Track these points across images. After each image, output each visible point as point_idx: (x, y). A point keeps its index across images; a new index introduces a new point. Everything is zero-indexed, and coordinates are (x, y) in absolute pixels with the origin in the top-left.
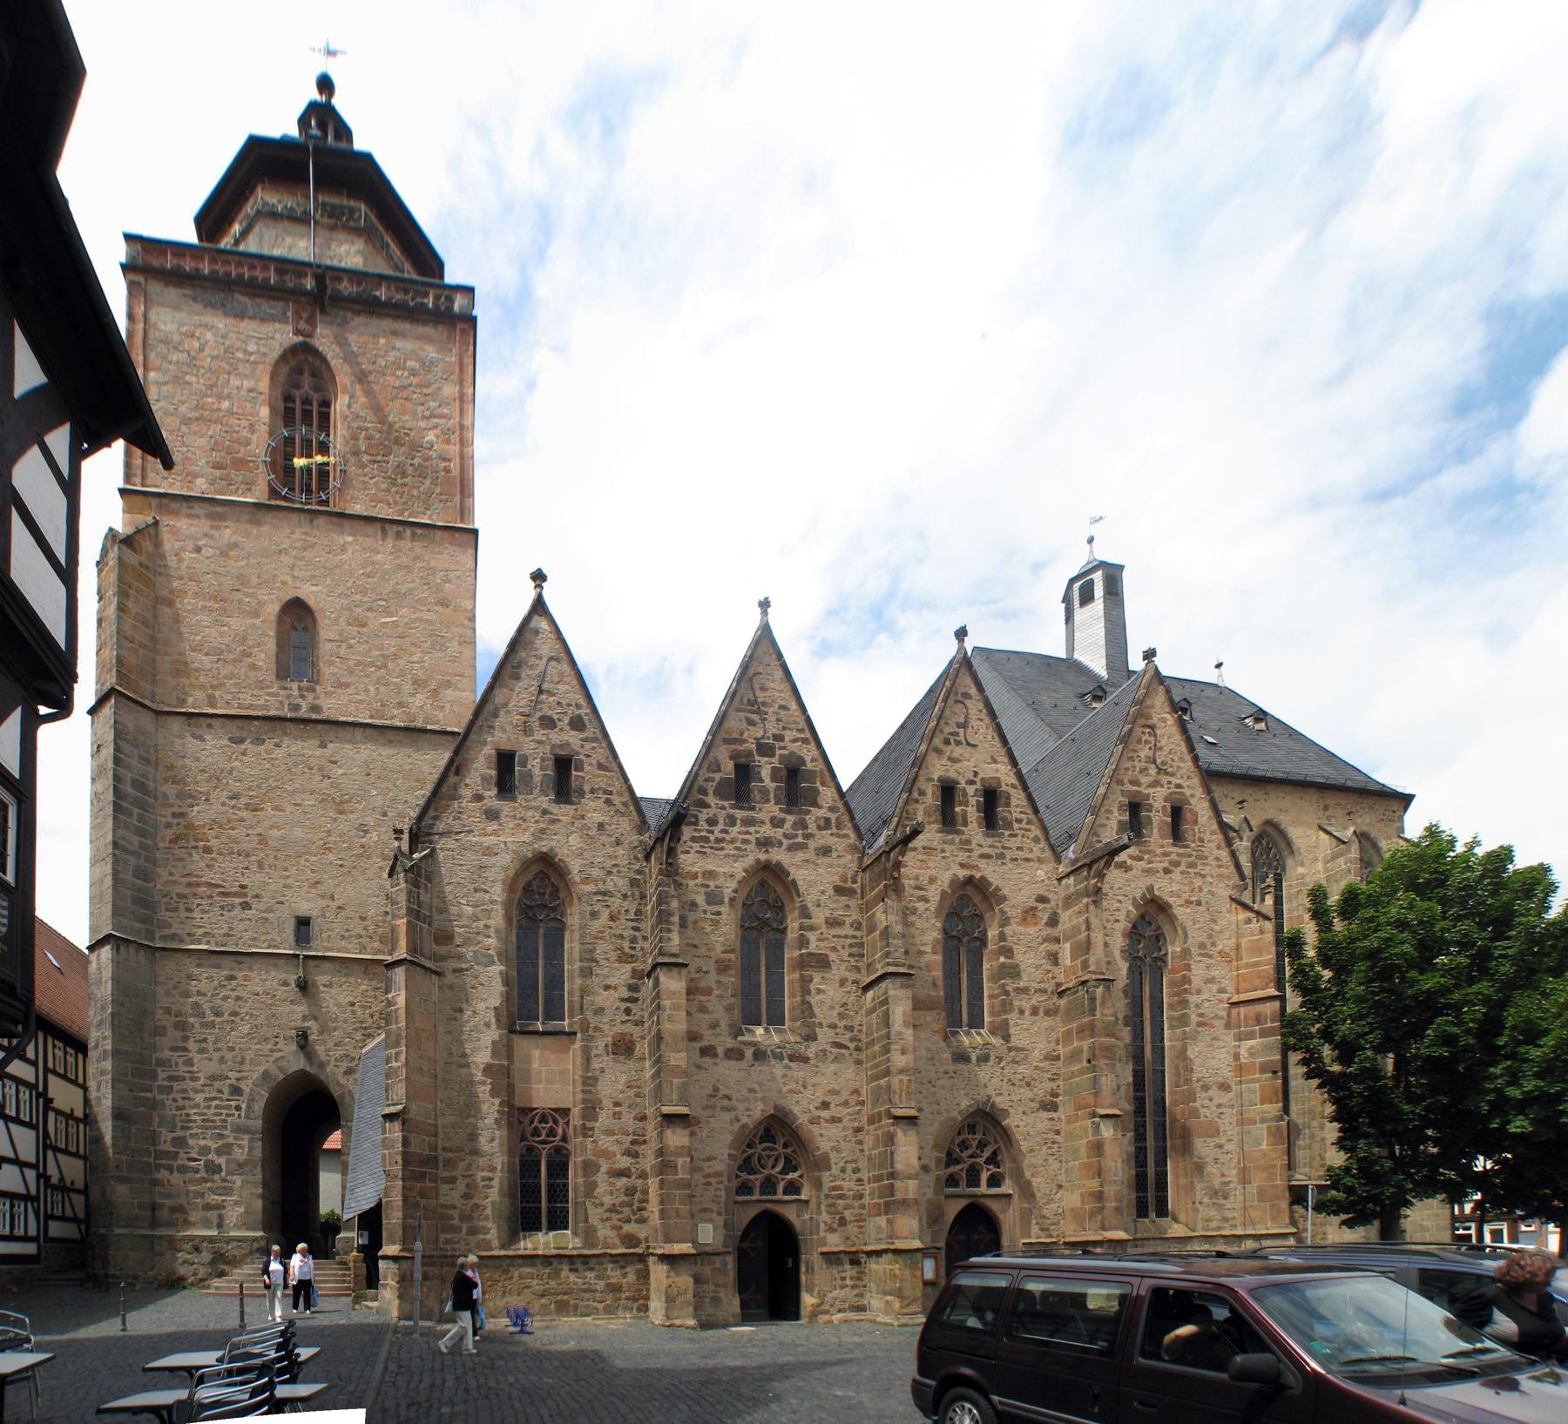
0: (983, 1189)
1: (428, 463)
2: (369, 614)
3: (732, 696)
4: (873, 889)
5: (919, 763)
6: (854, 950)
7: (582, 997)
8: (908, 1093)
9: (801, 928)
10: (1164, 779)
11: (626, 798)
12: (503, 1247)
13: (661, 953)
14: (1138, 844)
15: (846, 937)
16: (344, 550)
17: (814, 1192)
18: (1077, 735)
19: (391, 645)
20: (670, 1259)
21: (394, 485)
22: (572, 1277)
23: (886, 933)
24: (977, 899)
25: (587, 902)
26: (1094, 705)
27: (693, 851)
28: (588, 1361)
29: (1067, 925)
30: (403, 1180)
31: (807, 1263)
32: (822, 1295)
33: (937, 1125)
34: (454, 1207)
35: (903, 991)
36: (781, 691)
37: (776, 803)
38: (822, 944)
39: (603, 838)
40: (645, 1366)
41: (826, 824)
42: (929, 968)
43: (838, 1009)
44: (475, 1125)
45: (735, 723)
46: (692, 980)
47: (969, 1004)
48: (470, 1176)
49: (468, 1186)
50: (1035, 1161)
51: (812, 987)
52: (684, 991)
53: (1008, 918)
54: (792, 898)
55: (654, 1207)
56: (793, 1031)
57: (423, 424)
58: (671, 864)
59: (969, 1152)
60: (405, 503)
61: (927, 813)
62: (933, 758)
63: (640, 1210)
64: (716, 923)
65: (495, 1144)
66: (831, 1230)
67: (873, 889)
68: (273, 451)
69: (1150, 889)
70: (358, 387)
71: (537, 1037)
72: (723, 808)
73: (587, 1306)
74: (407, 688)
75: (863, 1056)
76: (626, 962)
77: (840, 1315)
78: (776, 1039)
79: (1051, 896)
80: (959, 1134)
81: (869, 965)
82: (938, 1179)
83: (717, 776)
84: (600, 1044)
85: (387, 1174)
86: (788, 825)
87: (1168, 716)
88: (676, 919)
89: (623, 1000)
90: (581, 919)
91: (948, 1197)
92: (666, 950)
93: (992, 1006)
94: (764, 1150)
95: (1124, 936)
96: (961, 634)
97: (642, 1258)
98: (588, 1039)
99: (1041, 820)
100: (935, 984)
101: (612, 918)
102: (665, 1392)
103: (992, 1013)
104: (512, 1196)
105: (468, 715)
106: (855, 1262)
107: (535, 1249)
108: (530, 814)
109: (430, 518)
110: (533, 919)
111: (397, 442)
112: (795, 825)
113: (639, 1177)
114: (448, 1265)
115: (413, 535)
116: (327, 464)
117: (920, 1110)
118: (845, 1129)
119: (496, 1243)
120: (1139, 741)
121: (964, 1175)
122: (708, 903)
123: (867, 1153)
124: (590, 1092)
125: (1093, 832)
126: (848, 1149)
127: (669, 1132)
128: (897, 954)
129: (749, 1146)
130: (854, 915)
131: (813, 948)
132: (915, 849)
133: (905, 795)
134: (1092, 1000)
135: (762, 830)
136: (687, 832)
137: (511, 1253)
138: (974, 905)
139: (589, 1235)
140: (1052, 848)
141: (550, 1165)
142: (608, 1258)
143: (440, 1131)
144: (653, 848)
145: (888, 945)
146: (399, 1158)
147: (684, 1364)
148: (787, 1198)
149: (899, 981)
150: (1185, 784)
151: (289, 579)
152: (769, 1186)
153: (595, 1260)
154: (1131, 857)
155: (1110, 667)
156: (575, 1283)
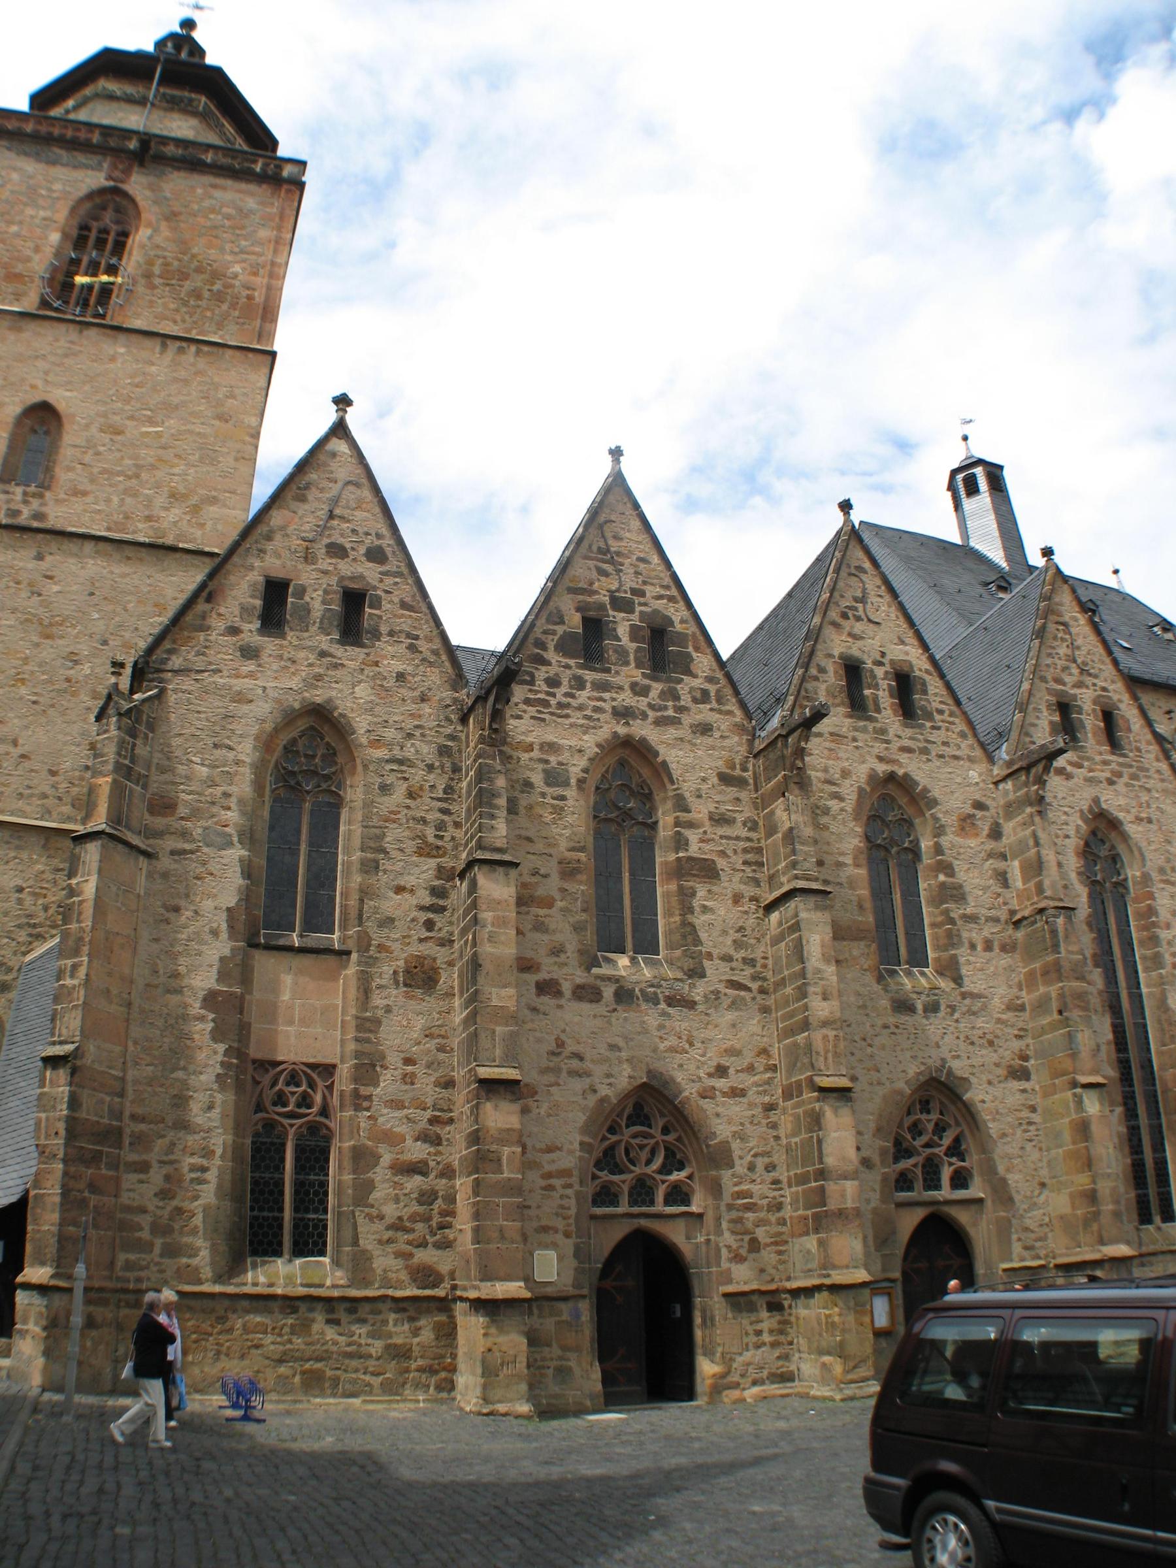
0: (945, 1192)
1: (229, 291)
2: (128, 423)
3: (577, 542)
5: (814, 636)
6: (749, 856)
7: (362, 901)
8: (836, 1055)
9: (677, 823)
10: (1089, 680)
11: (437, 644)
12: (218, 1279)
13: (480, 846)
14: (1075, 749)
15: (738, 838)
16: (113, 359)
17: (710, 1201)
18: (987, 624)
19: (148, 455)
20: (489, 1307)
21: (186, 306)
22: (331, 1333)
23: (790, 836)
24: (903, 801)
25: (376, 772)
26: (1001, 595)
27: (526, 716)
28: (355, 1469)
29: (1013, 838)
30: (65, 1161)
31: (704, 1311)
32: (727, 1360)
34: (143, 1210)
35: (819, 914)
36: (640, 543)
37: (638, 667)
38: (707, 847)
39: (402, 690)
40: (448, 1478)
41: (704, 697)
42: (852, 884)
43: (733, 935)
44: (185, 1085)
45: (582, 571)
46: (524, 885)
47: (907, 933)
48: (171, 1162)
49: (167, 1178)
50: (1009, 1150)
51: (696, 903)
52: (513, 901)
53: (942, 826)
54: (664, 786)
55: (464, 1224)
56: (671, 963)
57: (229, 258)
58: (496, 731)
59: (924, 1139)
60: (195, 322)
61: (829, 693)
62: (828, 631)
63: (442, 1227)
64: (559, 811)
65: (216, 1113)
66: (738, 1258)
67: (769, 780)
68: (54, 270)
69: (1096, 801)
70: (164, 224)
71: (289, 955)
72: (567, 667)
73: (354, 1382)
74: (160, 501)
75: (771, 1001)
76: (429, 855)
77: (756, 1390)
78: (647, 973)
79: (989, 802)
80: (909, 1113)
81: (771, 878)
82: (885, 1179)
83: (560, 630)
84: (385, 971)
85: (41, 1150)
86: (654, 694)
87: (1078, 615)
88: (502, 802)
90: (366, 793)
91: (900, 1205)
92: (485, 842)
93: (935, 937)
94: (635, 1136)
95: (1078, 854)
96: (846, 506)
97: (444, 1305)
98: (372, 962)
99: (964, 713)
100: (861, 907)
101: (411, 795)
102: (483, 1519)
103: (937, 948)
104: (237, 1198)
105: (234, 535)
106: (775, 1307)
107: (271, 1285)
108: (302, 654)
109: (221, 337)
110: (296, 789)
111: (199, 270)
112: (663, 695)
113: (442, 1175)
114: (128, 1305)
115: (198, 353)
116: (113, 283)
117: (854, 1079)
118: (751, 1105)
119: (207, 1272)
120: (1055, 638)
121: (919, 1171)
122: (548, 784)
123: (784, 1141)
124: (368, 1041)
125: (1024, 731)
126: (756, 1135)
127: (489, 1106)
128: (807, 865)
129: (612, 1130)
130: (748, 812)
131: (694, 850)
132: (819, 735)
133: (800, 672)
134: (1054, 932)
135: (621, 697)
136: (519, 692)
137: (230, 1289)
138: (900, 807)
139: (360, 1267)
140: (982, 745)
141: (299, 1150)
142: (389, 1304)
143: (130, 1089)
144: (472, 709)
145: (794, 852)
146: (61, 1127)
147: (512, 1474)
148: (670, 1210)
149: (812, 900)
150: (1111, 688)
151: (40, 383)
152: (642, 1191)
153: (367, 1307)
154: (1071, 763)
155: (1008, 558)
156: (335, 1343)
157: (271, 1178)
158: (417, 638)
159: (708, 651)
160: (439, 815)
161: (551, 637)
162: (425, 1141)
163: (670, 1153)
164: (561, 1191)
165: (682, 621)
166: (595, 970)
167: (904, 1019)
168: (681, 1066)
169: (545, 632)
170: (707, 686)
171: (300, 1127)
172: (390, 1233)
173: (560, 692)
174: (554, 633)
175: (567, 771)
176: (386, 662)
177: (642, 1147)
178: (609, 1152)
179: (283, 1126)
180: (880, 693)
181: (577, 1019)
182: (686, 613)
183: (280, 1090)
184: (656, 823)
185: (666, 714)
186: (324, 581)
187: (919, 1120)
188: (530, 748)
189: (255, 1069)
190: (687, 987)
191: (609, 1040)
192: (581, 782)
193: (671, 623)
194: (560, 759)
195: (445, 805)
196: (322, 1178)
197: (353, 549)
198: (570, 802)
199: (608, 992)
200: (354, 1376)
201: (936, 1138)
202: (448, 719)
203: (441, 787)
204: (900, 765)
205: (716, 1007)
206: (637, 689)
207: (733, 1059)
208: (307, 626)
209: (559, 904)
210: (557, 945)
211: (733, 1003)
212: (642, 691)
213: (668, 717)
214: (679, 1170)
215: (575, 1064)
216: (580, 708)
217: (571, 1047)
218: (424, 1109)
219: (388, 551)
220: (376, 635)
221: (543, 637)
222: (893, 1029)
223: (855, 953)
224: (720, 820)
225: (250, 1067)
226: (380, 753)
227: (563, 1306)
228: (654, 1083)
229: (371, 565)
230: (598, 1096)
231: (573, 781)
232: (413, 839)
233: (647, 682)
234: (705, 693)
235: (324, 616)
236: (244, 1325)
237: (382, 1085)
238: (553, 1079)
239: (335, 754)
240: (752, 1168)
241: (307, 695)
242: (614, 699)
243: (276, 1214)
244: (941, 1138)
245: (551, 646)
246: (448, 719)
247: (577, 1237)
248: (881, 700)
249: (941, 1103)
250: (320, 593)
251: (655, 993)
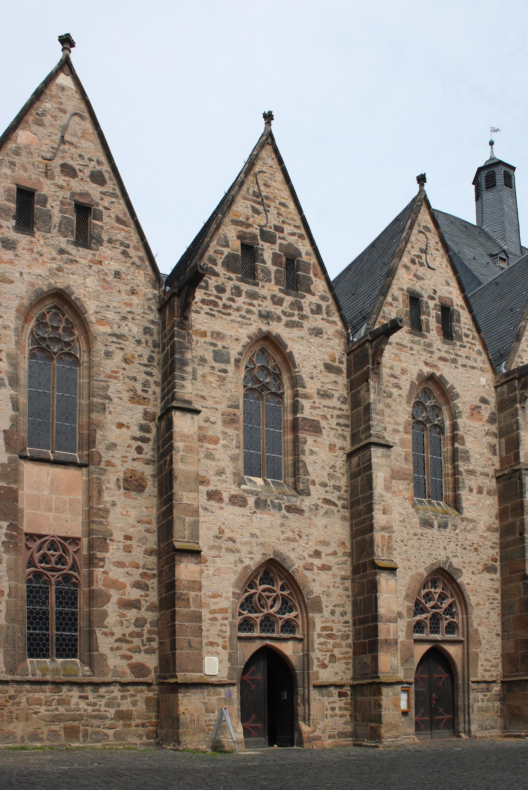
4: (358, 370)
15: (334, 408)
33: (408, 578)
37: (276, 284)
41: (318, 310)
59: (432, 603)
86: (286, 304)
89: (134, 438)
91: (416, 641)
112: (292, 305)
121: (428, 622)
157: (41, 609)
158: (128, 246)
159: (323, 277)
160: (145, 376)
161: (219, 256)
162: (139, 588)
163: (285, 601)
164: (221, 622)
165: (307, 254)
166: (243, 487)
167: (427, 531)
168: (294, 549)
169: (216, 252)
170: (321, 302)
171: (58, 577)
172: (118, 644)
173: (225, 296)
174: (222, 253)
175: (228, 353)
176: (106, 262)
177: (268, 597)
178: (249, 598)
179: (47, 576)
180: (431, 319)
181: (232, 516)
182: (309, 248)
183: (45, 553)
184: (283, 393)
185: (293, 319)
186: (61, 194)
187: (430, 592)
188: (204, 334)
189: (27, 539)
190: (299, 501)
191: (251, 531)
192: (237, 361)
193: (300, 255)
194: (224, 344)
195: (148, 369)
196: (73, 610)
197: (81, 171)
198: (230, 374)
199: (251, 500)
200: (97, 729)
201: (439, 603)
202: (150, 308)
203: (145, 357)
204: (439, 370)
205: (316, 515)
206: (276, 299)
207: (324, 547)
208: (50, 229)
209: (222, 442)
210: (220, 468)
211: (326, 513)
212: (279, 302)
213: (294, 322)
214: (290, 612)
215: (230, 544)
216: (238, 309)
217: (228, 534)
218: (138, 568)
219: (106, 175)
220: (100, 242)
221: (214, 256)
222: (419, 536)
223: (401, 487)
224: (325, 395)
225: (24, 538)
226: (106, 329)
227: (222, 690)
228: (278, 559)
229: (94, 185)
230: (244, 565)
231: (232, 360)
232: (128, 391)
233: (282, 295)
234: (319, 307)
235: (61, 221)
236: (28, 700)
237: (111, 551)
238: (217, 553)
239: (73, 327)
240: (333, 613)
241: (52, 281)
242: (260, 305)
243: (45, 632)
244: (441, 604)
245: (220, 262)
246: (150, 308)
247: (230, 649)
248: (431, 324)
249: (443, 583)
250: (59, 203)
251: (280, 504)
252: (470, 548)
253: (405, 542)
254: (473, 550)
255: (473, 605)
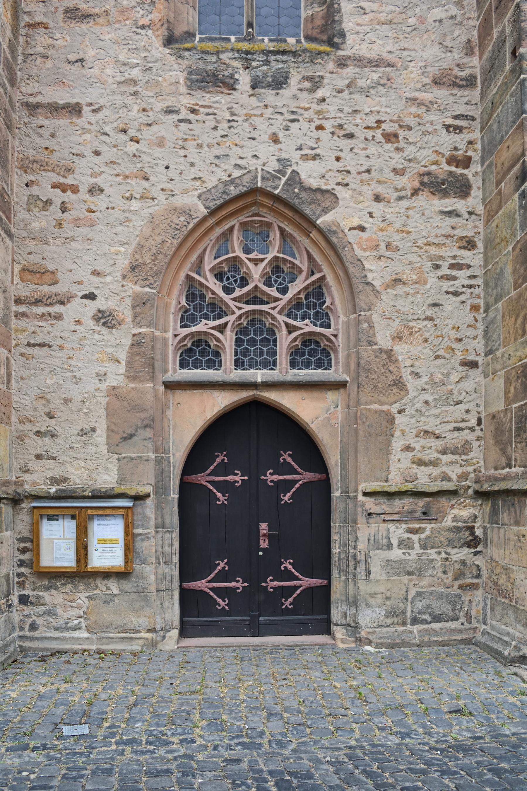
33: (138, 223)
222: (184, 114)
252: (369, 134)
253: (132, 133)
254: (379, 137)
255: (377, 284)
